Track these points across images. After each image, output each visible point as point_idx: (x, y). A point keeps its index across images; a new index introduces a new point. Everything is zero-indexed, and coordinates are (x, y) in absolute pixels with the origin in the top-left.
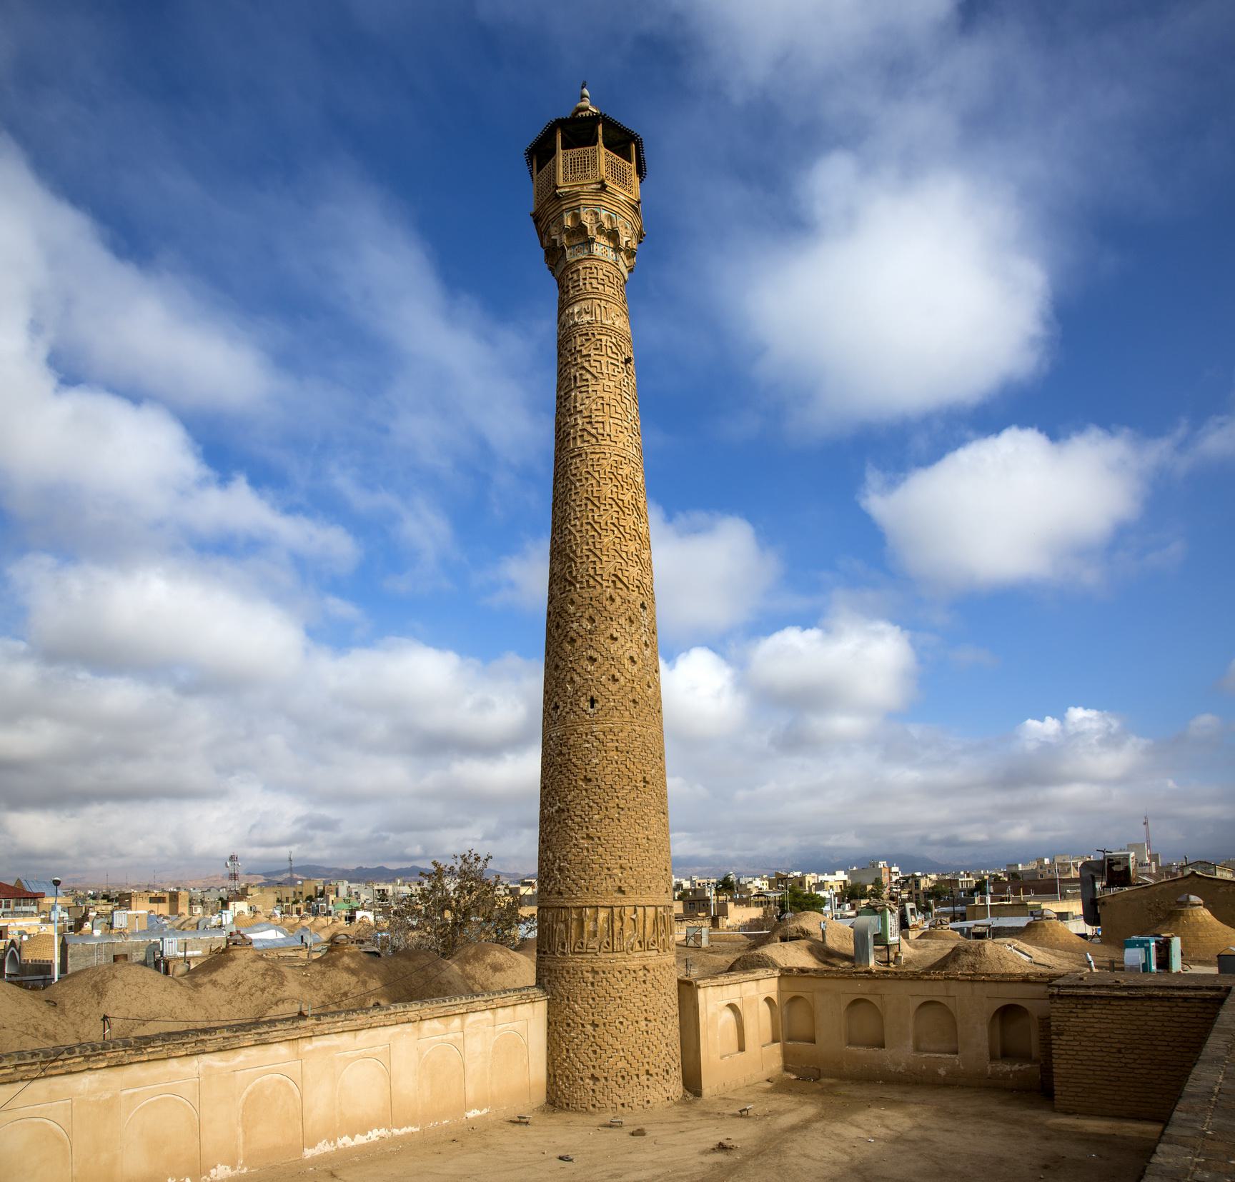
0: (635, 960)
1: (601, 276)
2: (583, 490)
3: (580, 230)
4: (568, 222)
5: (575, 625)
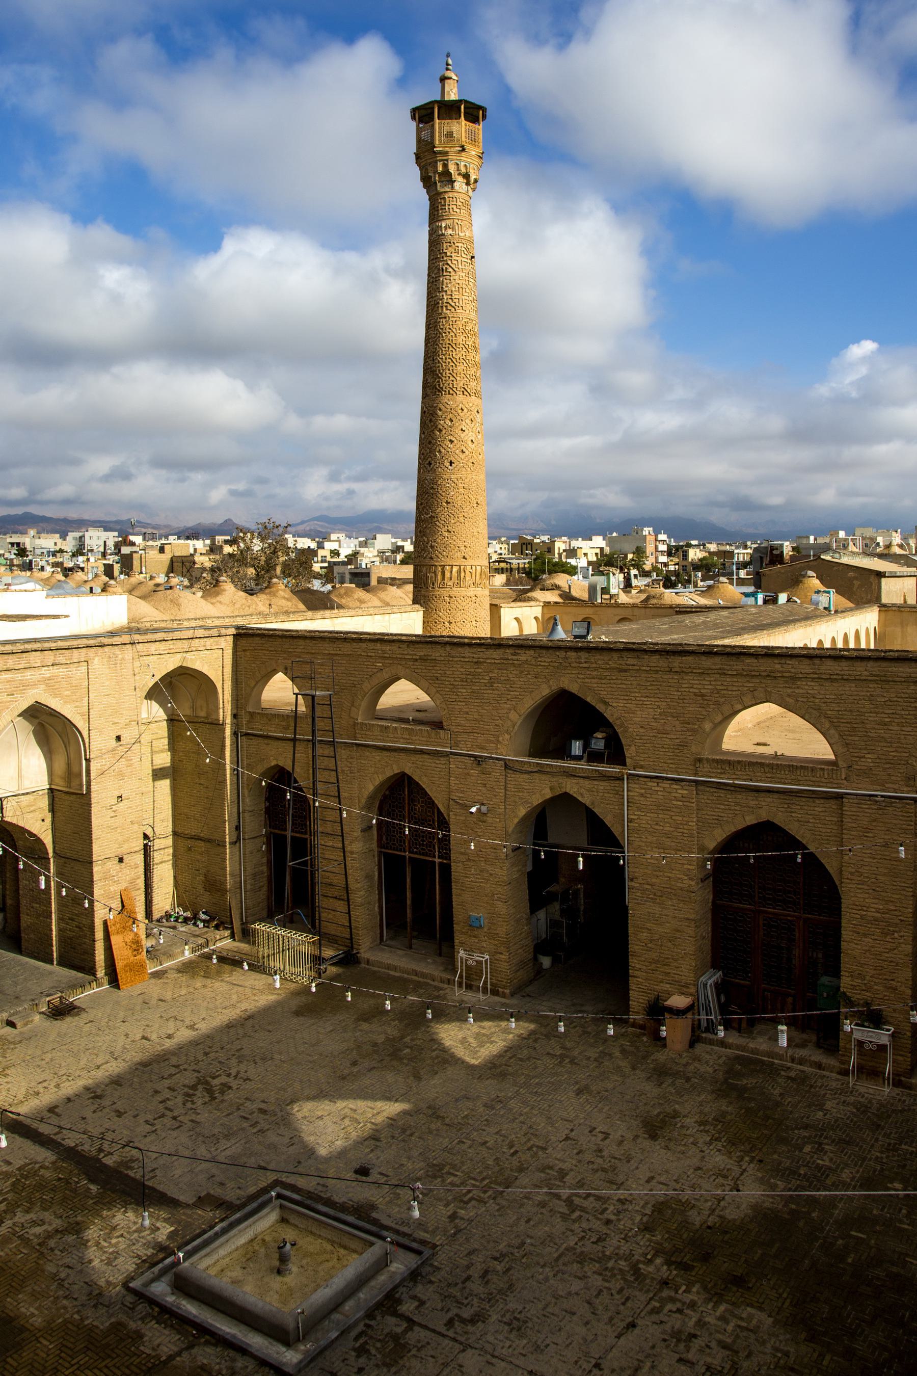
0: (472, 592)
1: (459, 203)
2: (447, 338)
3: (446, 174)
4: (440, 169)
5: (442, 422)
